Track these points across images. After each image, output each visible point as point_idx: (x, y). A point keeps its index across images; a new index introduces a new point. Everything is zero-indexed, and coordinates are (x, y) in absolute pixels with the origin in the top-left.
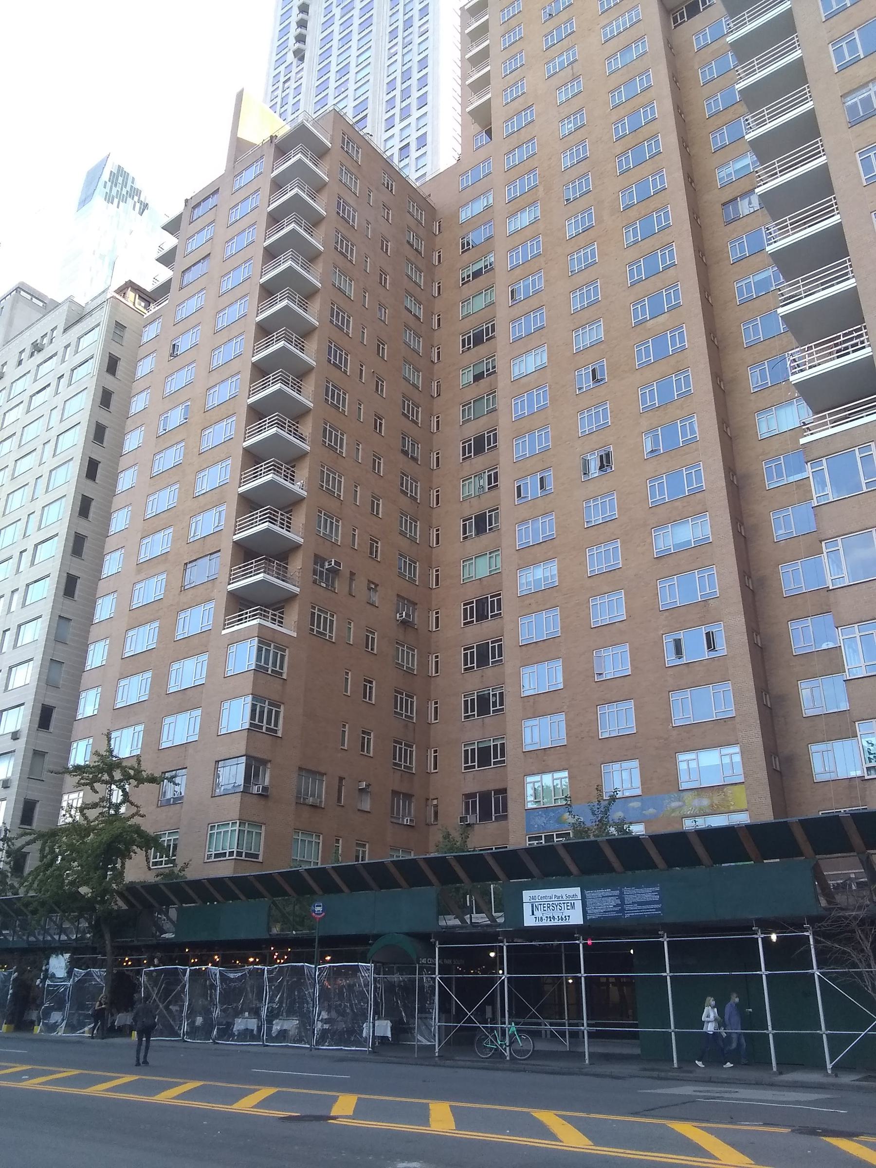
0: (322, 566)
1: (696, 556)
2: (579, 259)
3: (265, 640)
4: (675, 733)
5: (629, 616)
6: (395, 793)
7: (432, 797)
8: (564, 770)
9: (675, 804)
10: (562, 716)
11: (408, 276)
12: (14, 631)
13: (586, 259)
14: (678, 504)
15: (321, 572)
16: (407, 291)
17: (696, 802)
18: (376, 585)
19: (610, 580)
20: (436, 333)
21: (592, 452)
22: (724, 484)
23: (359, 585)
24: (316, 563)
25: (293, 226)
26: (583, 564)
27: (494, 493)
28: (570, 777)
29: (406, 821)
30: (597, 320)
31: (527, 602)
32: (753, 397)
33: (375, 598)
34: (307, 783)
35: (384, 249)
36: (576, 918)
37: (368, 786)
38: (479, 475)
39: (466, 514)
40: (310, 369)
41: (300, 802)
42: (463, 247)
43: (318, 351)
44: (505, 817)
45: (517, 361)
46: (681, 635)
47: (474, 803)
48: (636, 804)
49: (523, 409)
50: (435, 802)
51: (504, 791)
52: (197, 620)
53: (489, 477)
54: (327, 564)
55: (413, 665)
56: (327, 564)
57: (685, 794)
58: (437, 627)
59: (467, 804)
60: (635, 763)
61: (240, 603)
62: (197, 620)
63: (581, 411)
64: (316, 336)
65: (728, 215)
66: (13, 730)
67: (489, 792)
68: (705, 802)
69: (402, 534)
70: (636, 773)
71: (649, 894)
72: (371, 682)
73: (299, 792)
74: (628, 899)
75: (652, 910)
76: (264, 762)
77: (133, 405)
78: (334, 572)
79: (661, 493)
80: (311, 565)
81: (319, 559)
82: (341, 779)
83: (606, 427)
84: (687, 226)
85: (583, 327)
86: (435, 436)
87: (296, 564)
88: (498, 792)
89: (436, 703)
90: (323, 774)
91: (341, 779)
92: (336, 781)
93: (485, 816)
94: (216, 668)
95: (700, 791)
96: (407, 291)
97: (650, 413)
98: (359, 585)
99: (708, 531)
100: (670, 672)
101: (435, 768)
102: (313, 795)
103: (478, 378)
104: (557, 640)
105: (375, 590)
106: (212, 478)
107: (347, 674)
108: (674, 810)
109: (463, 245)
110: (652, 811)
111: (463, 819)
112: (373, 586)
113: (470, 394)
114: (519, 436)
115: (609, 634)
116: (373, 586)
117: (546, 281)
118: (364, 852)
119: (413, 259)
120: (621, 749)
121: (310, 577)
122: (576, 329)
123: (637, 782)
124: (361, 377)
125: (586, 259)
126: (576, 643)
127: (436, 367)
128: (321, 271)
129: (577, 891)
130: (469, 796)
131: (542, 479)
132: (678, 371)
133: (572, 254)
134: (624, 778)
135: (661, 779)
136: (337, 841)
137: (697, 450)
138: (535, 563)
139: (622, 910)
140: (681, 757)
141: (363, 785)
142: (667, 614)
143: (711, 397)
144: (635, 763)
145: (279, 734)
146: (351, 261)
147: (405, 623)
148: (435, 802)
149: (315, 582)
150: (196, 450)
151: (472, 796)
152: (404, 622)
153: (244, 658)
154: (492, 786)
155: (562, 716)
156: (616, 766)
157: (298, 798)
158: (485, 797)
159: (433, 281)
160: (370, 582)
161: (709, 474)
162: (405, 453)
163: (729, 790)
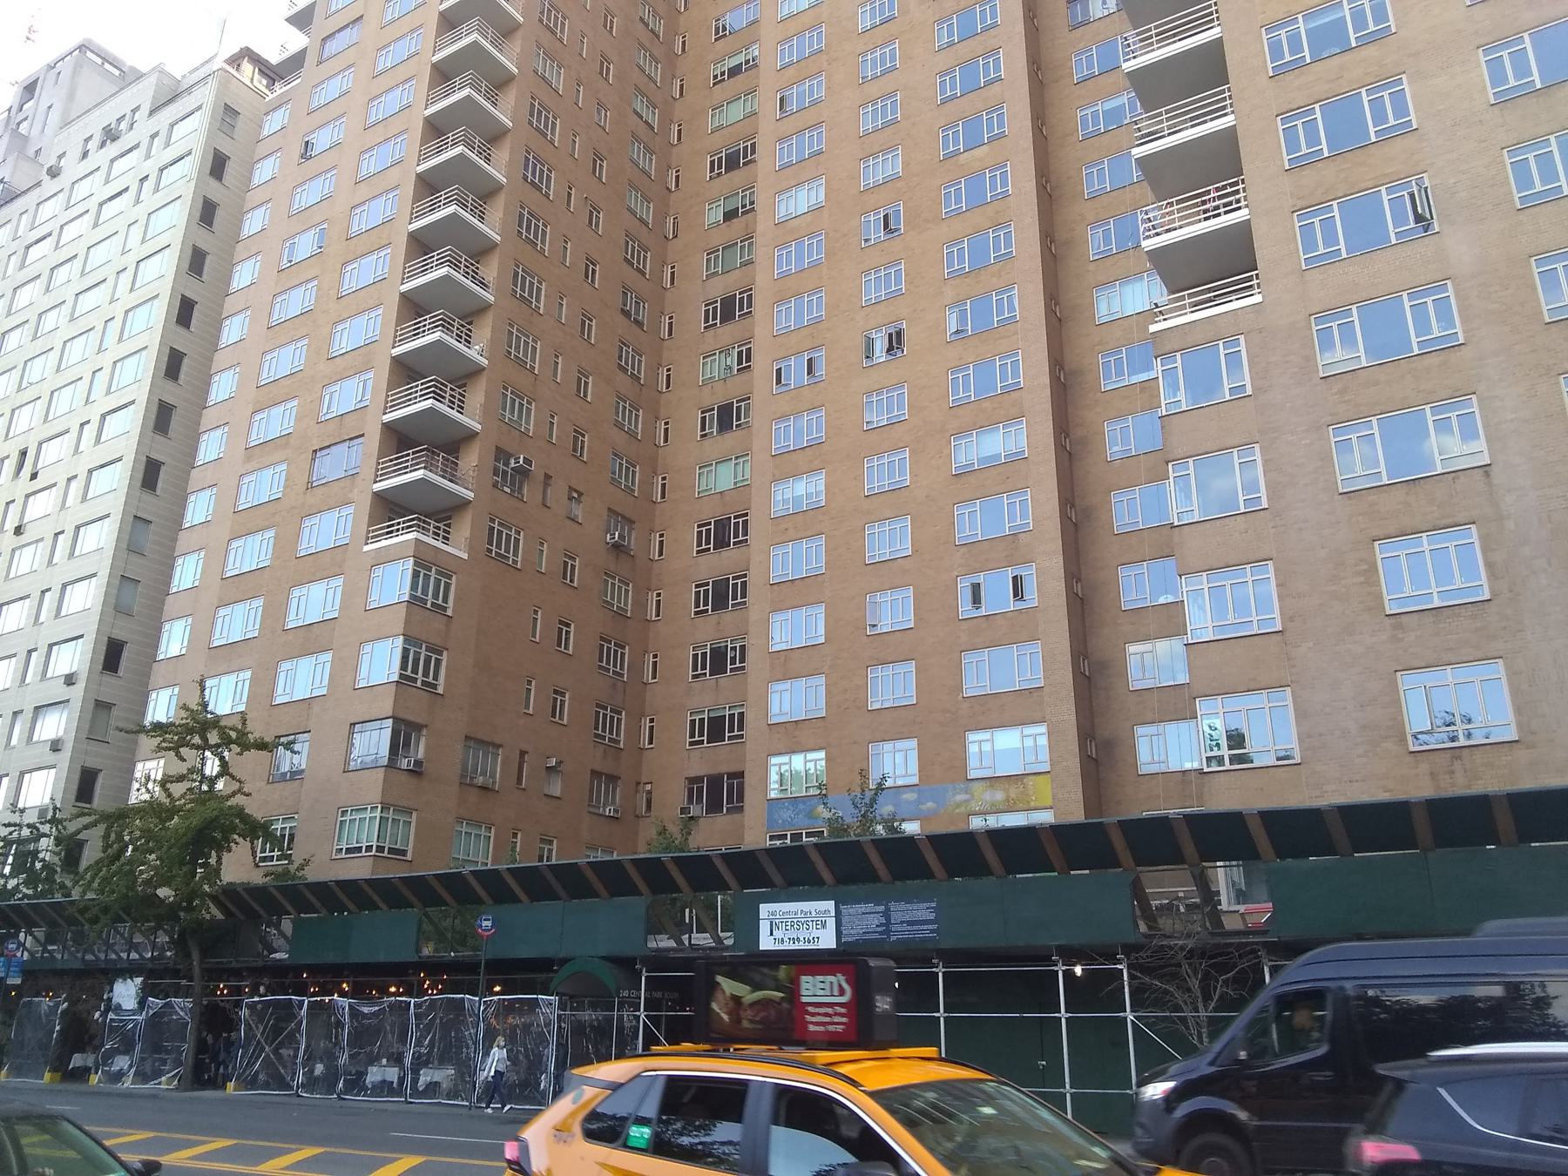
0: (507, 464)
1: (1003, 476)
2: (874, 61)
3: (423, 562)
4: (965, 705)
6: (595, 774)
7: (644, 780)
8: (820, 749)
9: (960, 797)
10: (822, 680)
11: (639, 67)
12: (43, 650)
13: (883, 63)
14: (986, 404)
15: (505, 473)
16: (637, 88)
17: (988, 796)
18: (580, 494)
19: (893, 502)
20: (675, 150)
21: (878, 328)
22: (1048, 381)
23: (557, 492)
24: (497, 459)
25: (474, 36)
26: (859, 478)
27: (745, 376)
28: (828, 759)
29: (609, 811)
30: (892, 148)
31: (783, 527)
32: (1092, 267)
33: (578, 511)
34: (476, 757)
35: (607, 26)
36: (827, 940)
37: (559, 763)
38: (726, 351)
39: (707, 403)
40: (493, 246)
41: (466, 782)
42: (717, 32)
43: (510, 163)
45: (784, 196)
46: (980, 578)
47: (700, 790)
48: (910, 796)
49: (789, 263)
50: (648, 787)
51: (741, 775)
52: (328, 530)
53: (740, 353)
55: (626, 604)
57: (976, 785)
58: (661, 554)
59: (691, 791)
60: (913, 743)
61: (390, 509)
62: (328, 530)
63: (867, 272)
64: (507, 144)
65: (1074, 16)
66: (53, 736)
68: (999, 796)
69: (620, 426)
70: (913, 757)
71: (923, 911)
72: (568, 625)
73: (464, 769)
74: (896, 917)
75: (926, 931)
76: (418, 728)
77: (236, 276)
78: (522, 473)
79: (966, 388)
80: (490, 462)
81: (502, 454)
82: (523, 753)
83: (896, 295)
84: (1020, 27)
85: (874, 155)
86: (668, 294)
87: (470, 460)
88: (732, 776)
89: (655, 656)
91: (523, 753)
93: (714, 807)
94: (354, 596)
95: (993, 781)
96: (637, 88)
97: (958, 280)
98: (557, 492)
99: (1024, 443)
100: (964, 625)
101: (651, 742)
102: (484, 773)
103: (730, 215)
104: (820, 579)
105: (578, 501)
106: (347, 396)
107: (536, 612)
108: (958, 805)
109: (717, 30)
110: (930, 805)
111: (683, 810)
112: (575, 495)
113: (718, 239)
114: (781, 300)
115: (888, 574)
116: (575, 495)
117: (828, 88)
118: (550, 851)
120: (896, 723)
121: (489, 478)
122: (865, 158)
123: (914, 767)
125: (883, 63)
126: (844, 584)
127: (673, 196)
128: (518, 50)
129: (830, 905)
130: (692, 780)
131: (810, 360)
132: (997, 225)
133: (864, 54)
134: (897, 763)
135: (945, 763)
136: (515, 835)
137: (1016, 333)
138: (796, 474)
139: (888, 932)
140: (972, 737)
141: (553, 762)
142: (963, 550)
143: (1037, 262)
144: (913, 743)
145: (440, 690)
146: (552, 142)
147: (617, 548)
148: (648, 787)
149: (495, 485)
150: (333, 293)
151: (699, 779)
153: (393, 584)
154: (724, 768)
155: (822, 680)
156: (888, 746)
157: (463, 776)
158: (715, 782)
159: (674, 77)
161: (1029, 367)
162: (626, 314)
163: (1030, 781)
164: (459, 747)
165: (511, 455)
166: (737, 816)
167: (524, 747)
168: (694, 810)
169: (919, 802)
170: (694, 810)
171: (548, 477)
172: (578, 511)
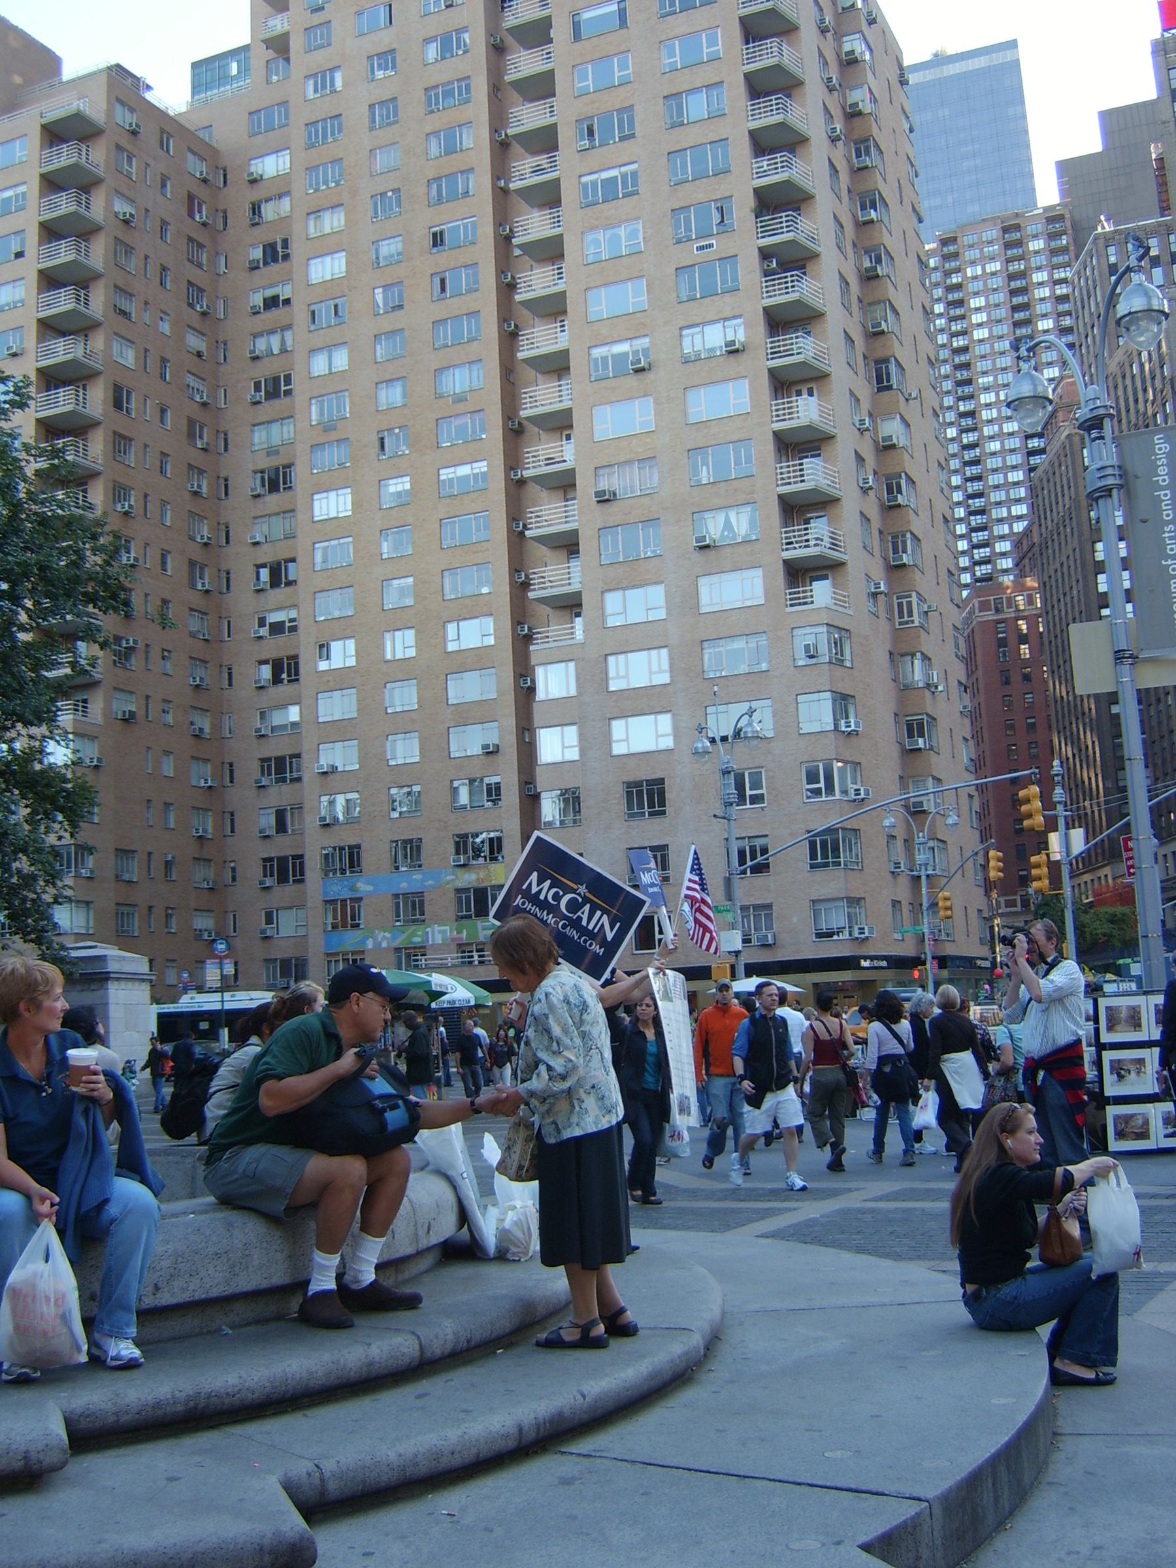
5: (420, 706)
18: (169, 652)
19: (403, 670)
23: (155, 653)
31: (325, 679)
44: (301, 881)
47: (272, 866)
50: (232, 865)
51: (301, 857)
54: (124, 642)
56: (124, 642)
67: (287, 858)
88: (294, 857)
90: (133, 852)
91: (150, 854)
92: (145, 857)
93: (283, 879)
115: (403, 724)
119: (194, 235)
124: (145, 413)
131: (336, 306)
148: (232, 865)
152: (197, 686)
154: (289, 852)
158: (282, 860)
160: (164, 650)
164: (112, 857)
165: (122, 638)
166: (300, 886)
167: (149, 849)
168: (268, 882)
169: (423, 881)
170: (268, 882)
171: (147, 646)
172: (168, 665)
